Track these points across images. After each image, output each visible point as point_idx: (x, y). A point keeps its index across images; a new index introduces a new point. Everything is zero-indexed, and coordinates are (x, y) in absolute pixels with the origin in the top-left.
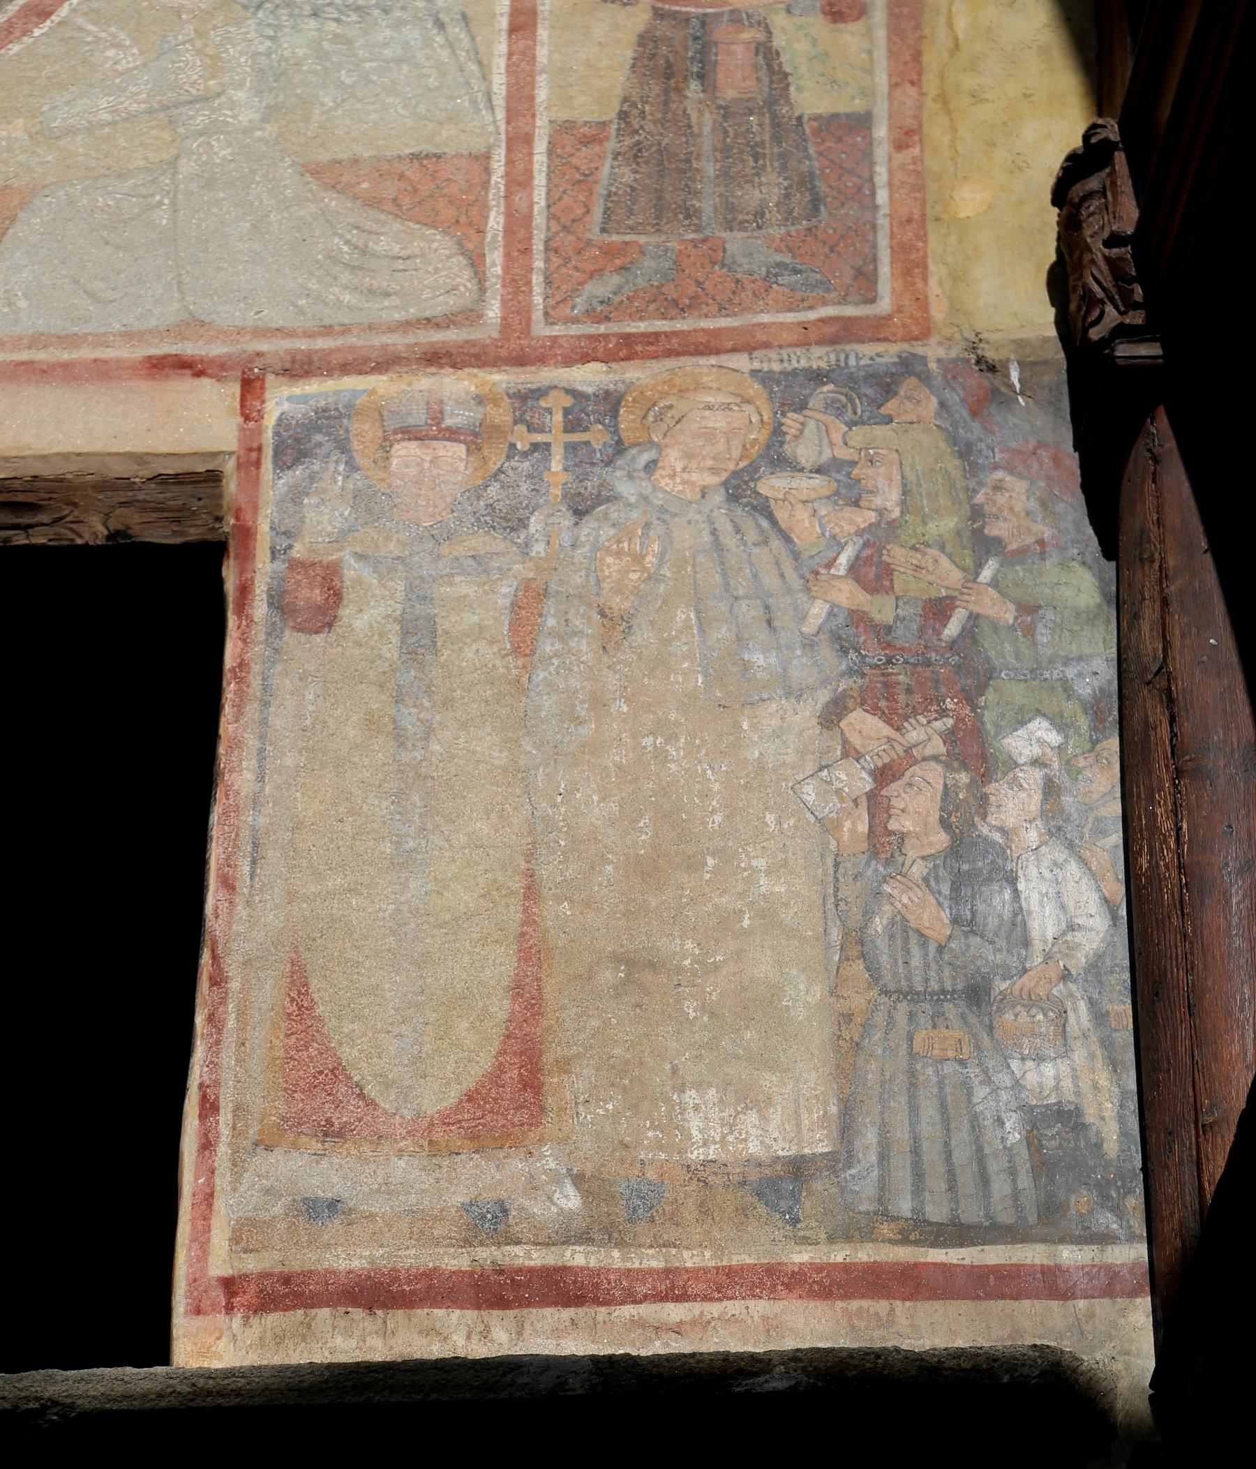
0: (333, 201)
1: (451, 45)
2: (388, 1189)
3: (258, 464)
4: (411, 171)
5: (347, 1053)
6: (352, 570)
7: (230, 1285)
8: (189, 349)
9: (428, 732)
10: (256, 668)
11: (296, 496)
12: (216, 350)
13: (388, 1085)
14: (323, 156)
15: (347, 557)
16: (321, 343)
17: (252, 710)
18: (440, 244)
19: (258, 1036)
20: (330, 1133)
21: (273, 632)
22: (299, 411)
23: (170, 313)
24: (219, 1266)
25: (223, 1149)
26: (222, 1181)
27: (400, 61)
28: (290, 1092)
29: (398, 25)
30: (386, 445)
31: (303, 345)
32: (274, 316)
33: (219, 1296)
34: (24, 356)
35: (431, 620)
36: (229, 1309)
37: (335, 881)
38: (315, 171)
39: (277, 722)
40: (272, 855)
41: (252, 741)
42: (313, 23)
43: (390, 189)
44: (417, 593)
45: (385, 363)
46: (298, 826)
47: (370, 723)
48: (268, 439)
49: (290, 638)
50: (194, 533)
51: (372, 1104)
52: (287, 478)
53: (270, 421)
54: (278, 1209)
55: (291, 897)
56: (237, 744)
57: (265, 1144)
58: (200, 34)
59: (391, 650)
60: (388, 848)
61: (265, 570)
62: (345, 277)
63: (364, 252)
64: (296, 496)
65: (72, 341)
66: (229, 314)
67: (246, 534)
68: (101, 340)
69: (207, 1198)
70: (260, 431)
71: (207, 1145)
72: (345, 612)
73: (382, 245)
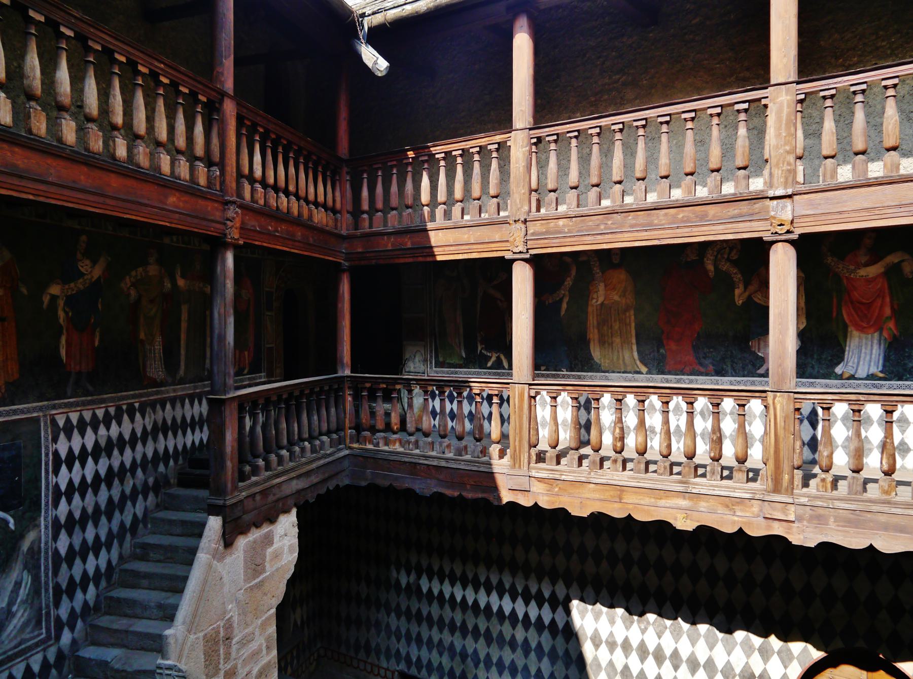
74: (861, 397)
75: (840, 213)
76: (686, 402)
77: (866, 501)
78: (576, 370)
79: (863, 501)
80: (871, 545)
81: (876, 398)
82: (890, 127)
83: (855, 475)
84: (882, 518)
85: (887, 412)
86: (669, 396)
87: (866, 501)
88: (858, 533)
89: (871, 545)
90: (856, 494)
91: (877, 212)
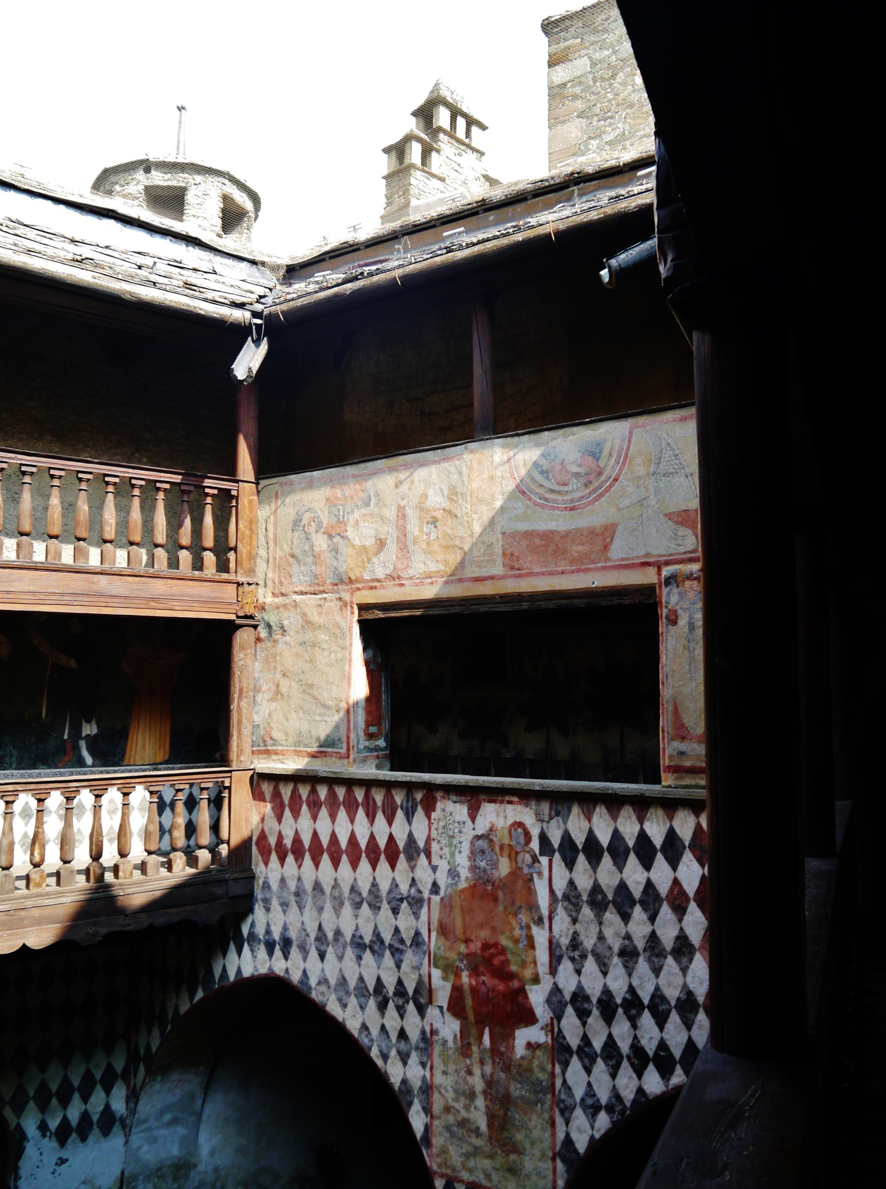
0: (671, 523)
1: (689, 481)
2: (693, 750)
3: (661, 586)
4: (684, 515)
5: (685, 721)
6: (679, 612)
7: (669, 767)
8: (648, 560)
9: (694, 649)
10: (664, 634)
11: (668, 594)
12: (652, 560)
13: (692, 728)
14: (667, 512)
15: (678, 608)
16: (671, 558)
17: (664, 643)
18: (689, 532)
19: (670, 717)
20: (683, 738)
21: (667, 626)
22: (668, 574)
23: (643, 553)
24: (667, 764)
25: (666, 740)
26: (666, 746)
27: (680, 486)
28: (676, 729)
29: (679, 477)
30: (684, 582)
31: (667, 558)
32: (662, 552)
33: (667, 769)
34: (620, 563)
35: (693, 623)
36: (669, 772)
37: (681, 683)
38: (666, 515)
39: (669, 647)
40: (670, 678)
41: (665, 652)
42: (664, 478)
43: (680, 519)
44: (691, 618)
45: (681, 562)
46: (673, 671)
47: (684, 647)
48: (663, 580)
49: (670, 627)
50: (652, 601)
51: (689, 732)
52: (668, 588)
53: (663, 576)
54: (675, 753)
55: (673, 687)
56: (662, 652)
57: (672, 739)
58: (644, 482)
59: (686, 630)
60: (689, 676)
61: (665, 611)
62: (673, 542)
63: (676, 534)
64: (668, 594)
65: (627, 559)
66: (655, 552)
67: (661, 602)
68: (633, 559)
69: (664, 749)
70: (661, 578)
71: (663, 739)
72: (679, 621)
73: (680, 533)
74: (19, 787)
75: (8, 592)
76: (37, 799)
77: (20, 898)
78: (60, 766)
79: (16, 899)
80: (24, 945)
81: (86, 784)
82: (55, 516)
83: (6, 872)
84: (36, 913)
85: (68, 799)
86: (16, 793)
87: (20, 898)
88: (11, 935)
89: (24, 945)
90: (7, 893)
91: (42, 597)
